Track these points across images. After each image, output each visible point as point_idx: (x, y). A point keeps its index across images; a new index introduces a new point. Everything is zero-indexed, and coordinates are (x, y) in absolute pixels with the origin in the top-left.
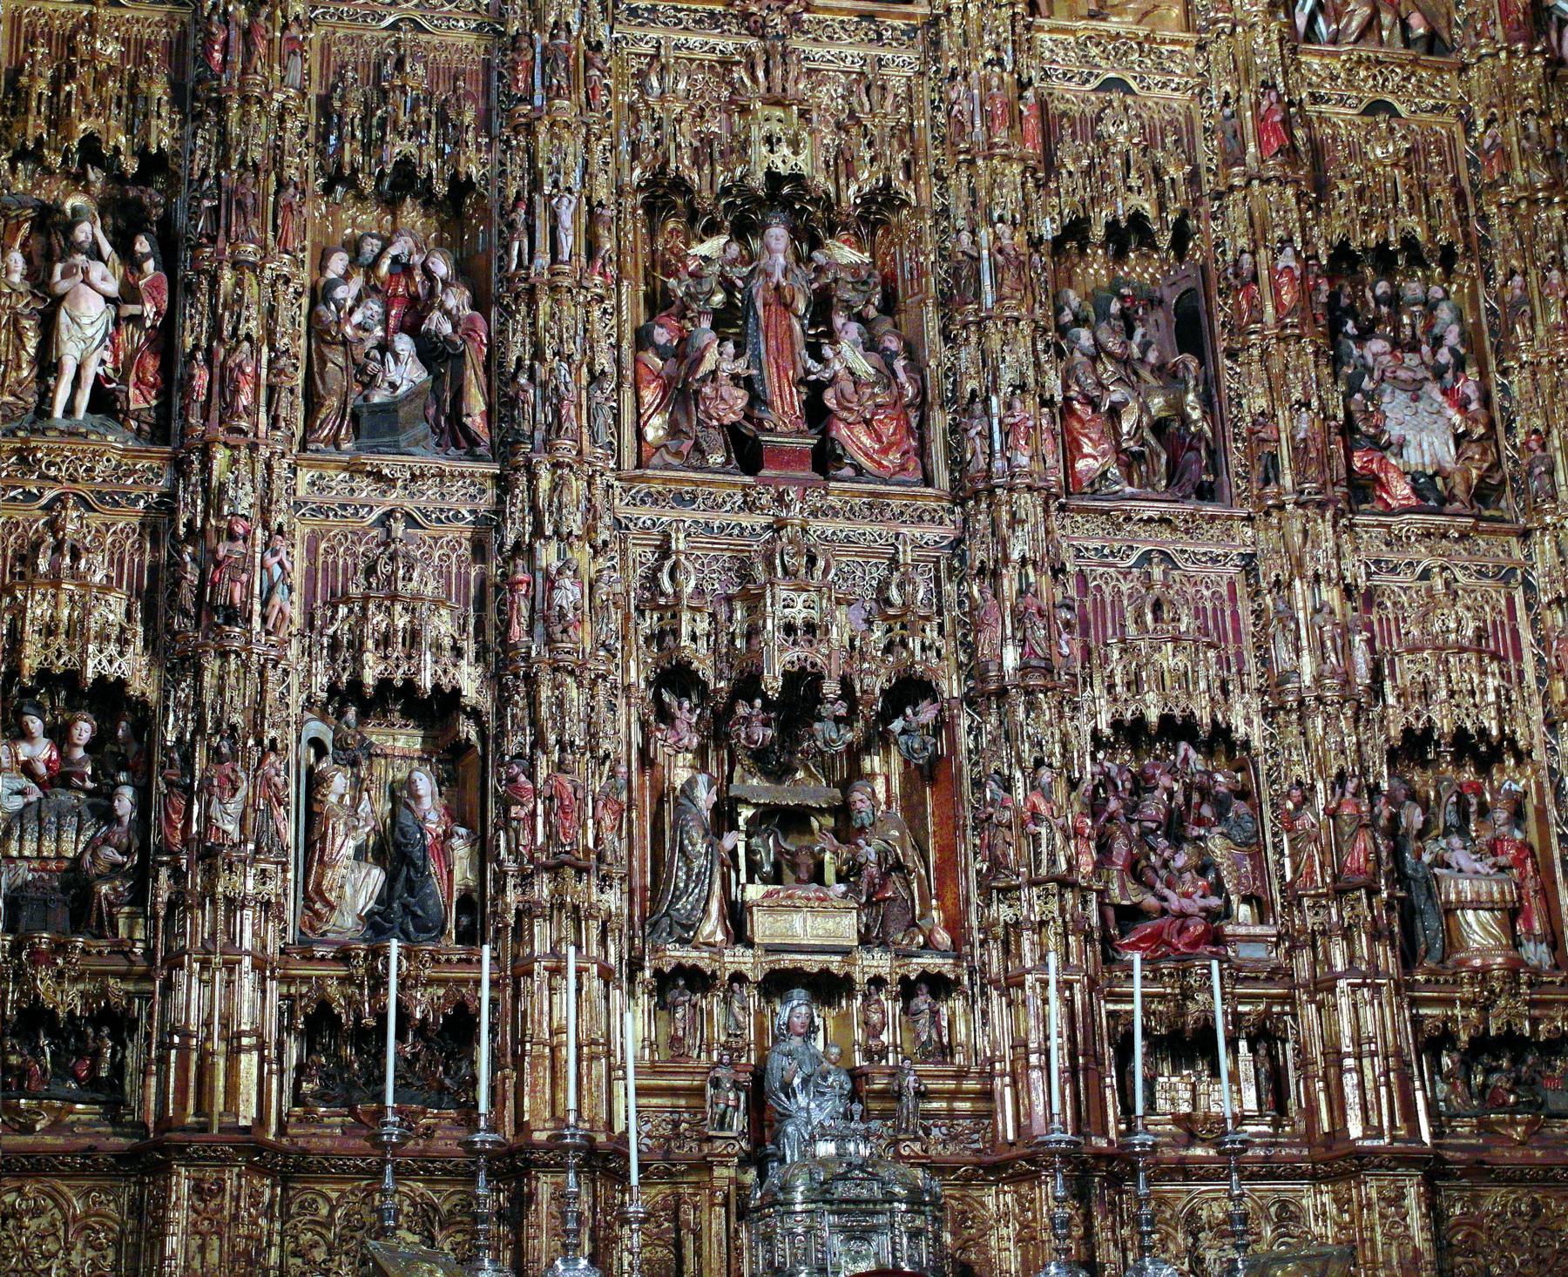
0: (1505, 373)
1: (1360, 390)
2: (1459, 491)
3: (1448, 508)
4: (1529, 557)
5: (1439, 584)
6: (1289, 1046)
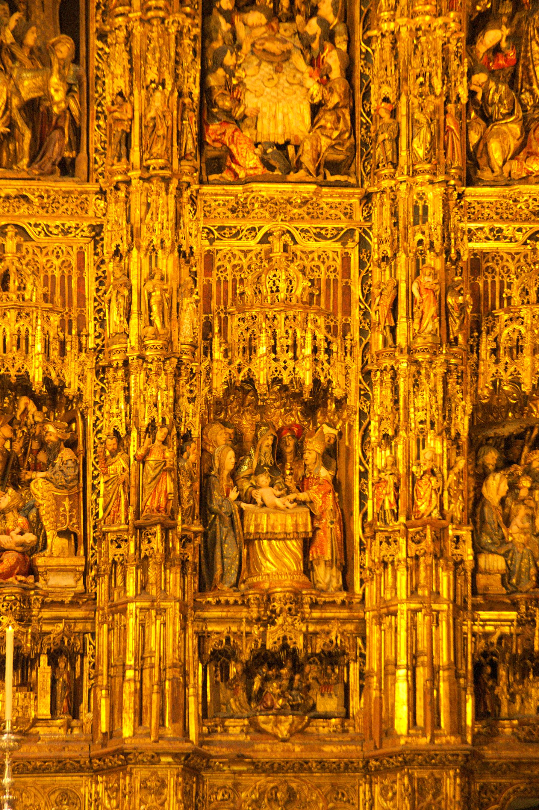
0: (368, 41)
1: (222, 65)
2: (307, 159)
3: (292, 176)
4: (368, 218)
5: (277, 246)
6: (86, 660)
